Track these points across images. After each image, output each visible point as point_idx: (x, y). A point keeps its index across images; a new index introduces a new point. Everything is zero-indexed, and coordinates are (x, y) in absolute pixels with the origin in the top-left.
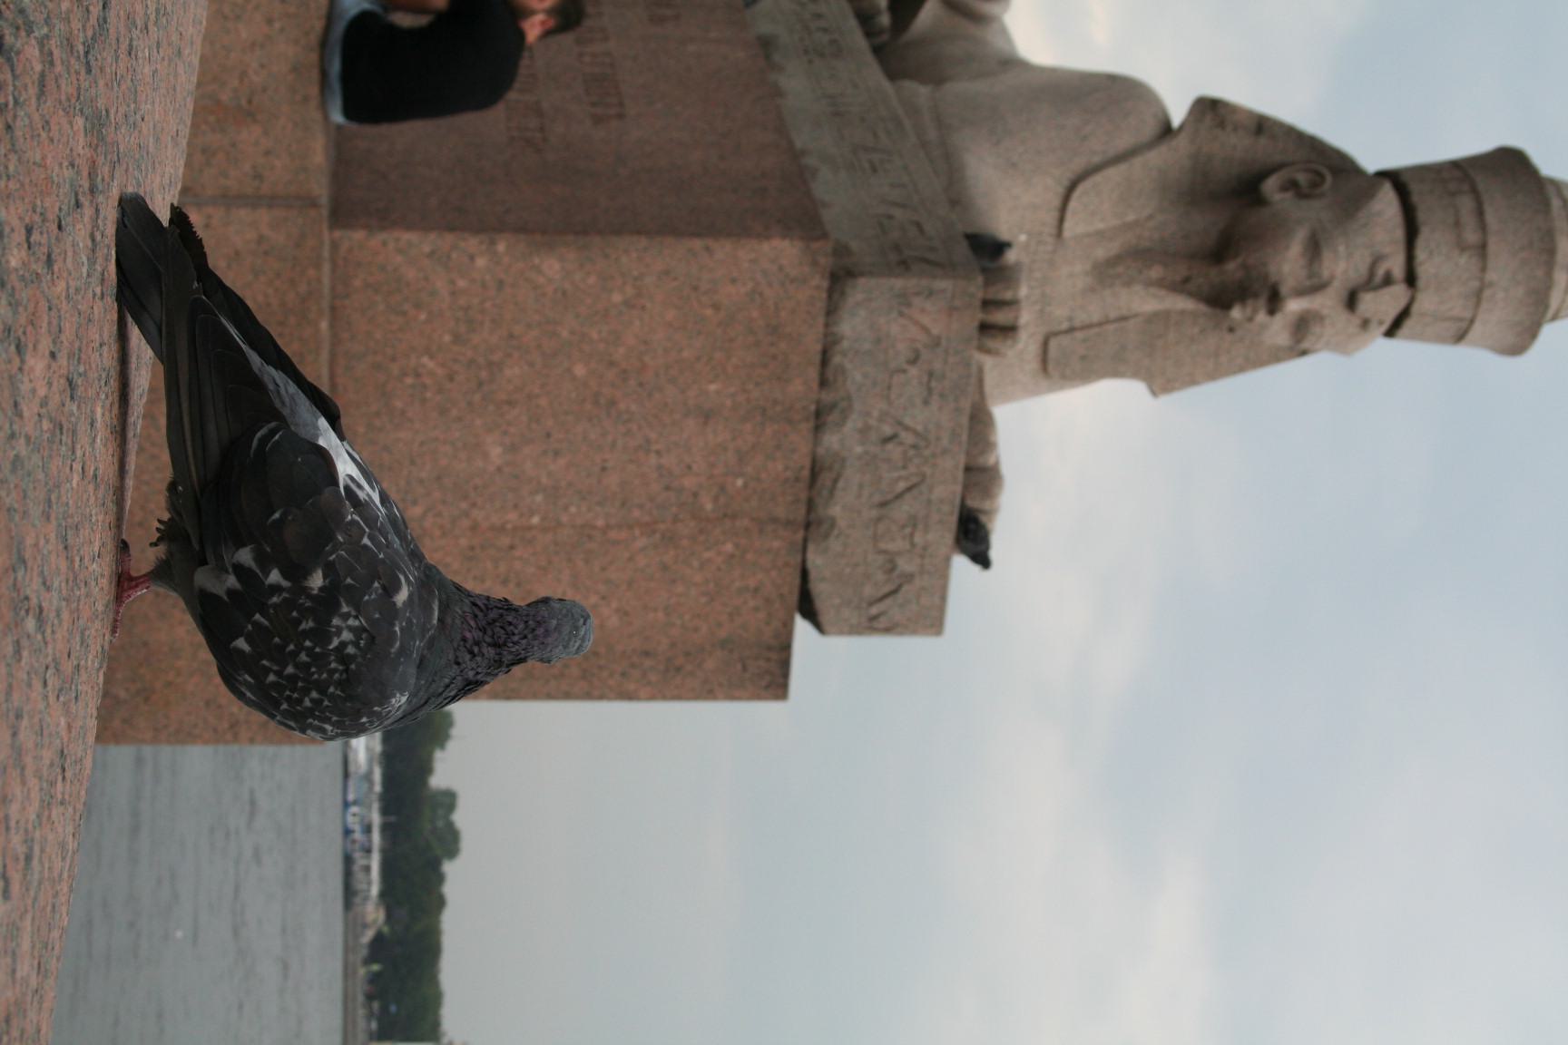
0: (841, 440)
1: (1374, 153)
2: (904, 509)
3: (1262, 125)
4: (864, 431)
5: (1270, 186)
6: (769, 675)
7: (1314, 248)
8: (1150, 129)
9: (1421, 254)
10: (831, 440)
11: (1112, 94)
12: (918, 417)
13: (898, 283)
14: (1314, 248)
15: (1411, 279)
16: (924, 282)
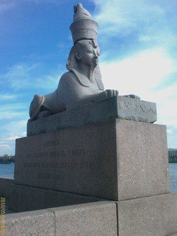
0: (136, 117)
1: (72, 44)
2: (144, 109)
3: (70, 59)
4: (135, 114)
5: (78, 58)
6: (163, 128)
7: (90, 52)
8: (71, 74)
9: (88, 38)
10: (137, 119)
11: (64, 81)
12: (133, 106)
13: (118, 108)
14: (90, 52)
15: (92, 39)
16: (118, 105)
